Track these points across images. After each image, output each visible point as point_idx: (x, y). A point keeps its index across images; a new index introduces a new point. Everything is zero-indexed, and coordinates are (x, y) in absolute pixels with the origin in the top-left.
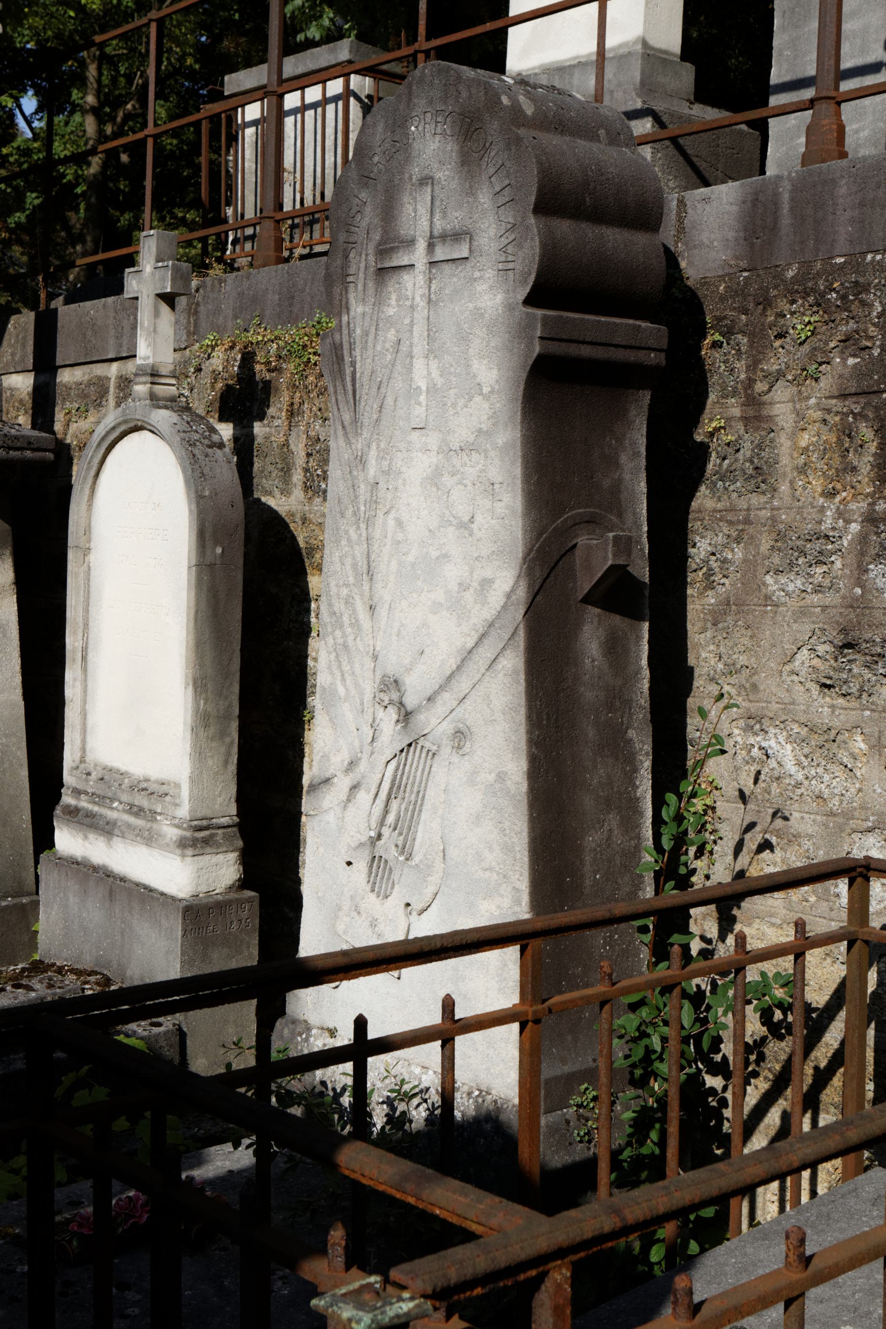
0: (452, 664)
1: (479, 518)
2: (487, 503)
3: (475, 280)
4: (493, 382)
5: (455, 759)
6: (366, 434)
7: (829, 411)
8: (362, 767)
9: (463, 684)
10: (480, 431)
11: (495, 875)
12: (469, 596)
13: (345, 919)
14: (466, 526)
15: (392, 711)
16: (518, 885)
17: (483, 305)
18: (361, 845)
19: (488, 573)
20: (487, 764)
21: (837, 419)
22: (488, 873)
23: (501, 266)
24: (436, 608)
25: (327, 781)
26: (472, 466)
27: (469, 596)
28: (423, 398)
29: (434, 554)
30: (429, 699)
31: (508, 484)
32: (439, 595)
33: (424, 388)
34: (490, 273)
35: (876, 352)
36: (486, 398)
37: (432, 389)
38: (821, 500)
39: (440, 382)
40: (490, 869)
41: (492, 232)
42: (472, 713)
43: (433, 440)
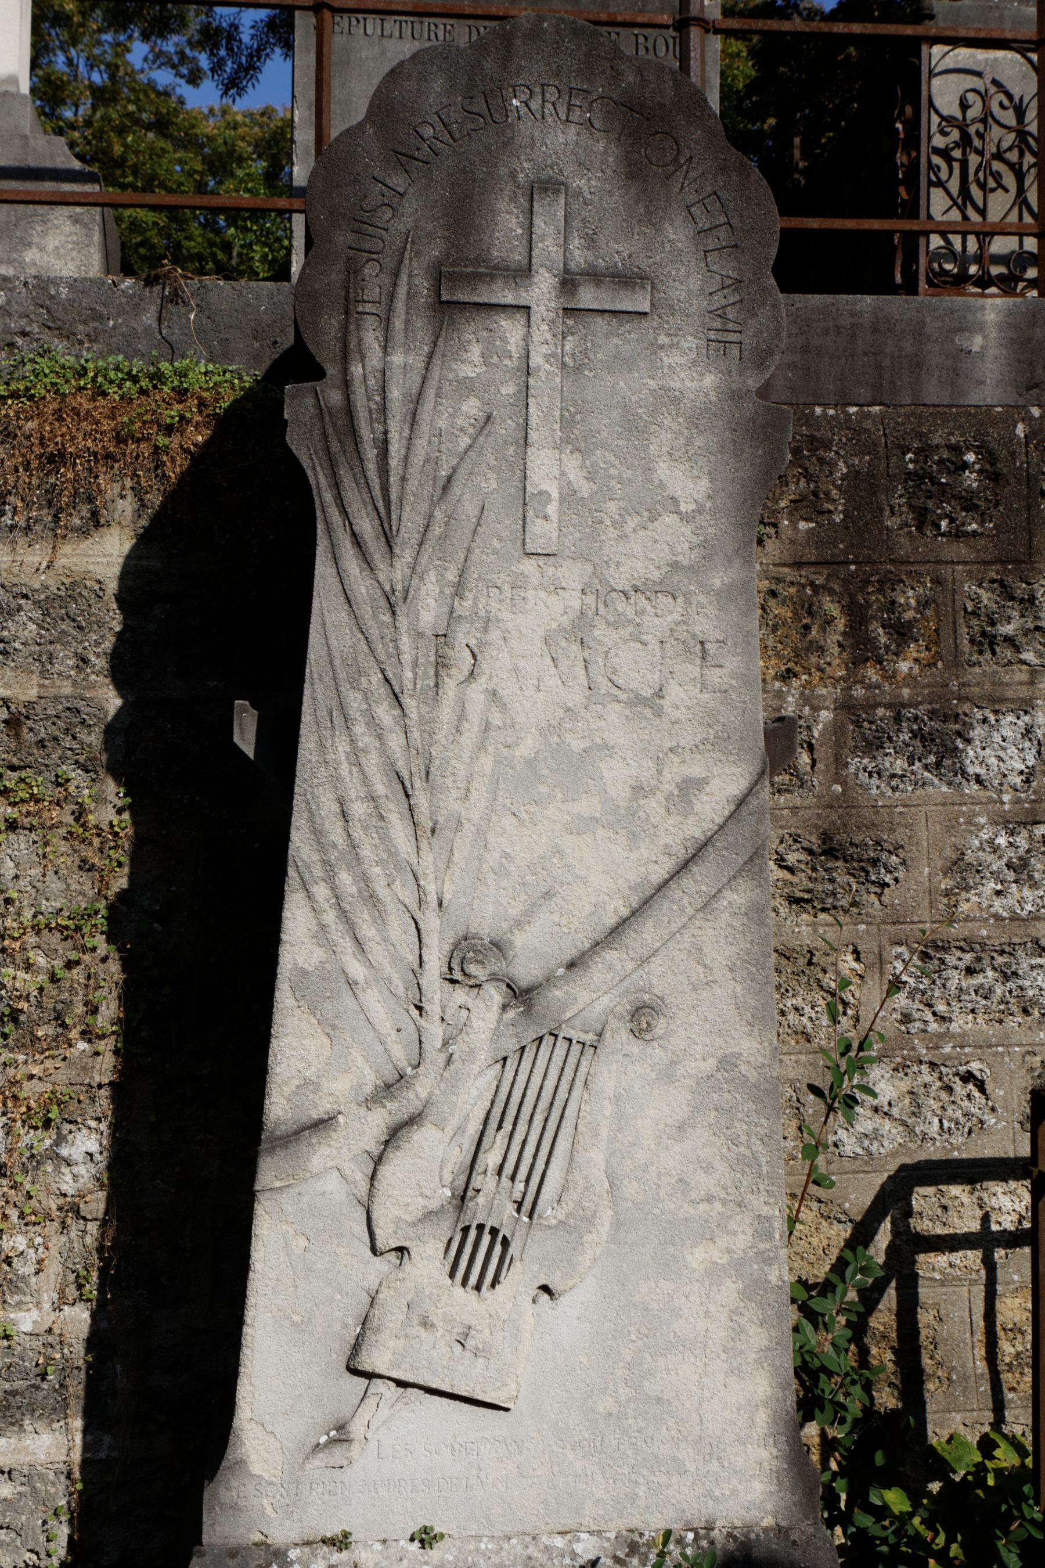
0: (616, 909)
1: (674, 692)
3: (662, 347)
4: (700, 497)
5: (635, 1047)
6: (406, 556)
7: (778, 580)
8: (423, 1087)
9: (649, 933)
10: (675, 566)
11: (718, 1206)
12: (653, 806)
13: (391, 1344)
14: (651, 702)
15: (493, 991)
16: (765, 1211)
17: (677, 385)
18: (428, 1216)
19: (696, 771)
20: (699, 1048)
21: (792, 590)
22: (703, 1207)
23: (712, 335)
24: (581, 826)
25: (323, 1124)
26: (661, 617)
27: (653, 806)
28: (552, 509)
29: (577, 744)
30: (571, 965)
31: (735, 644)
32: (586, 806)
33: (555, 495)
34: (689, 342)
35: (838, 518)
36: (685, 518)
37: (569, 497)
38: (777, 684)
39: (585, 489)
40: (709, 1199)
41: (694, 283)
42: (660, 978)
43: (572, 574)
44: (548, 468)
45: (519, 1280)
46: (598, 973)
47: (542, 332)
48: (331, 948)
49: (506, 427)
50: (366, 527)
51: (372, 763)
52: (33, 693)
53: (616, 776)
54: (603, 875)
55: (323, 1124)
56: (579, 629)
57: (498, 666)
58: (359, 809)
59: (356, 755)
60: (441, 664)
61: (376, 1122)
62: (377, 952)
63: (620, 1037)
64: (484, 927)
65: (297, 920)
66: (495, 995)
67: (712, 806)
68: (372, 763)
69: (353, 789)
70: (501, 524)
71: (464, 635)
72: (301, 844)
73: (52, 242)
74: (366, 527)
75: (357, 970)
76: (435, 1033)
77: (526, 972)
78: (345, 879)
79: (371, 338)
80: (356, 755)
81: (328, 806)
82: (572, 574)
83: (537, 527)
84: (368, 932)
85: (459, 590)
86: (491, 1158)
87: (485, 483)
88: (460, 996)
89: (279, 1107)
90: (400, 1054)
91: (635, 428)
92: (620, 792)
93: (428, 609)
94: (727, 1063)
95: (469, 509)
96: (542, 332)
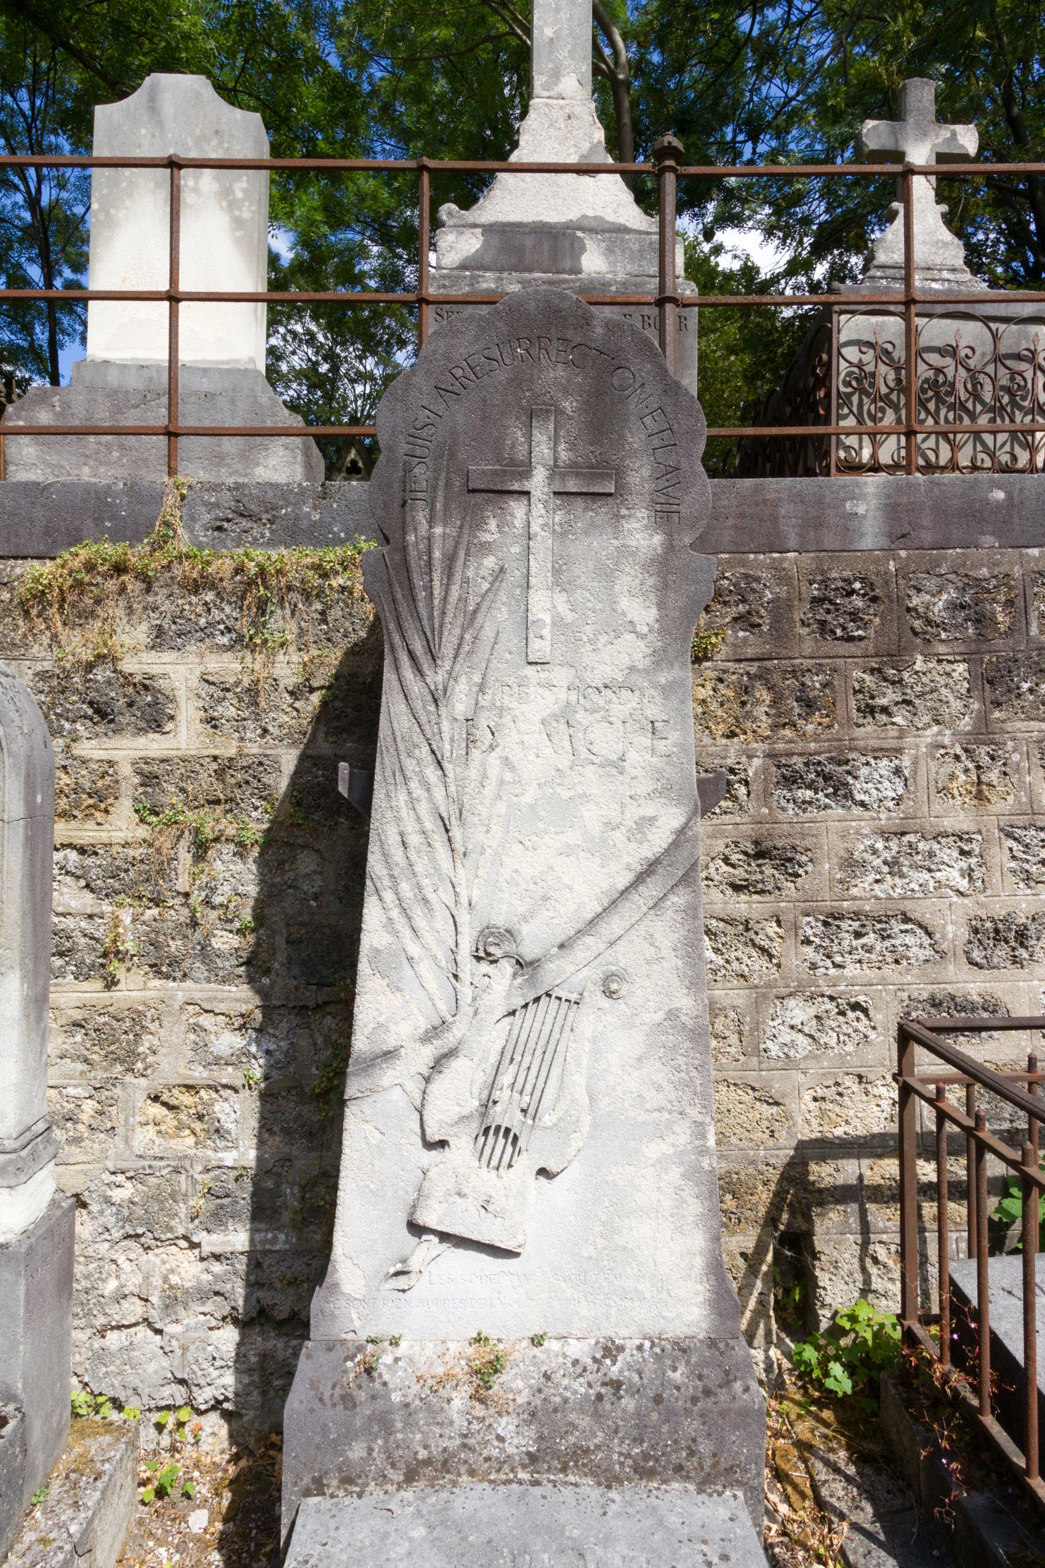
0: (594, 907)
1: (633, 756)
2: (646, 741)
3: (623, 517)
4: (651, 620)
5: (606, 1003)
6: (447, 665)
7: (724, 672)
8: (458, 1031)
9: (615, 925)
10: (632, 669)
11: (667, 1115)
12: (618, 837)
13: (436, 1206)
14: (618, 764)
15: (506, 965)
16: (700, 1118)
17: (634, 543)
18: (463, 1119)
19: (649, 811)
20: (651, 1004)
21: (734, 677)
22: (656, 1114)
23: (658, 507)
24: (567, 852)
25: (389, 1055)
26: (623, 705)
27: (618, 837)
28: (546, 632)
29: (565, 794)
30: (562, 946)
31: (676, 723)
32: (572, 837)
33: (548, 621)
34: (642, 513)
35: (765, 628)
36: (642, 636)
37: (558, 622)
38: (724, 741)
39: (570, 617)
40: (660, 1110)
41: (646, 472)
42: (624, 956)
43: (561, 676)
44: (544, 604)
45: (526, 1164)
46: (581, 953)
47: (538, 509)
48: (396, 933)
49: (515, 575)
50: (418, 647)
51: (423, 808)
52: (232, 752)
53: (592, 817)
54: (585, 883)
55: (389, 1055)
56: (566, 716)
57: (509, 740)
58: (414, 839)
59: (412, 802)
60: (470, 741)
61: (428, 1053)
62: (428, 937)
63: (596, 998)
64: (500, 921)
65: (372, 914)
66: (507, 967)
67: (660, 839)
68: (423, 808)
69: (410, 826)
70: (511, 641)
71: (483, 721)
72: (374, 862)
73: (272, 461)
74: (418, 647)
75: (414, 950)
76: (466, 993)
77: (529, 951)
78: (405, 887)
79: (421, 517)
80: (412, 802)
81: (392, 838)
82: (561, 676)
83: (536, 644)
84: (421, 923)
85: (482, 688)
86: (506, 1079)
87: (499, 617)
88: (485, 967)
89: (361, 1043)
90: (444, 1007)
91: (607, 574)
92: (594, 827)
93: (461, 702)
94: (672, 1015)
95: (488, 632)
96: (538, 509)
